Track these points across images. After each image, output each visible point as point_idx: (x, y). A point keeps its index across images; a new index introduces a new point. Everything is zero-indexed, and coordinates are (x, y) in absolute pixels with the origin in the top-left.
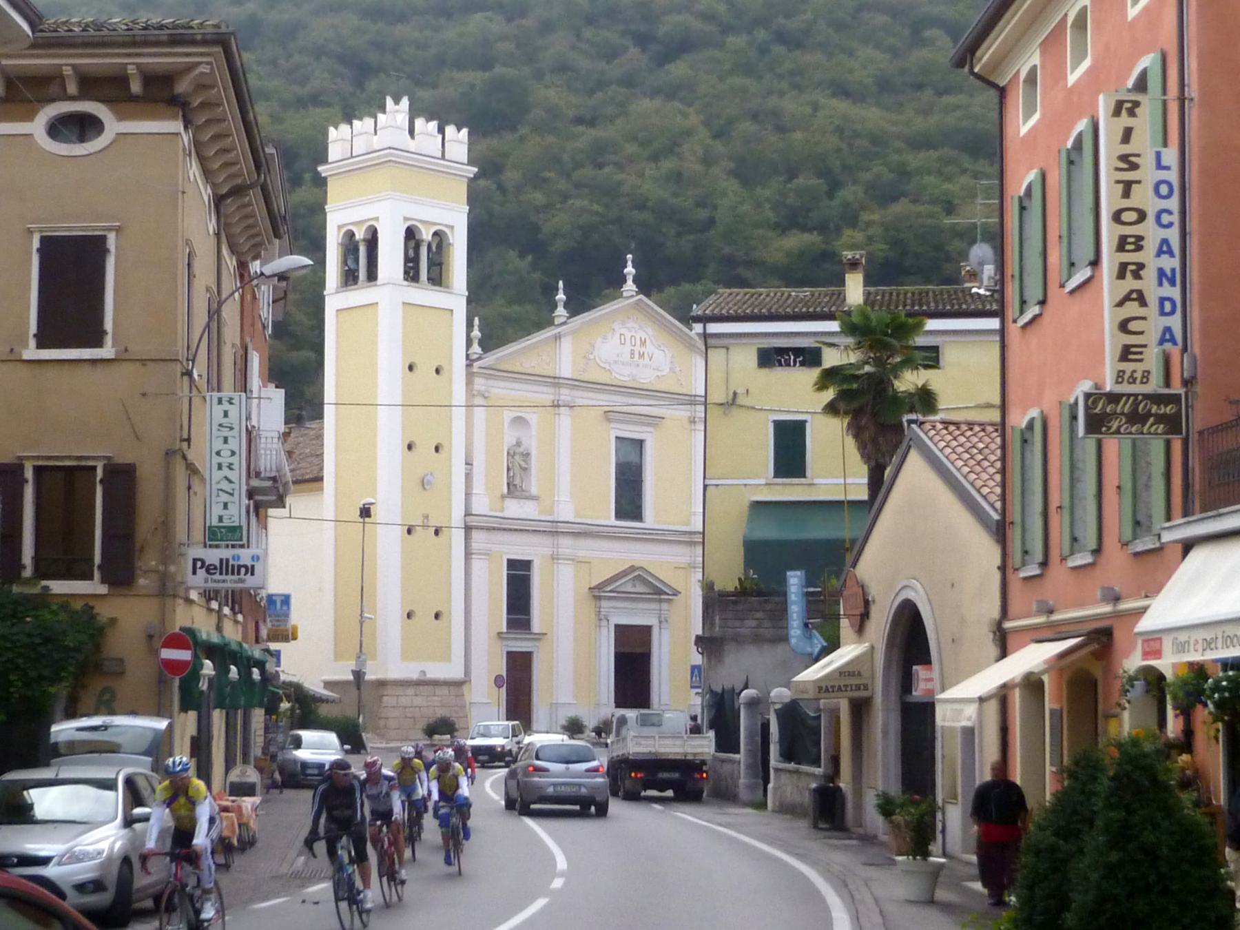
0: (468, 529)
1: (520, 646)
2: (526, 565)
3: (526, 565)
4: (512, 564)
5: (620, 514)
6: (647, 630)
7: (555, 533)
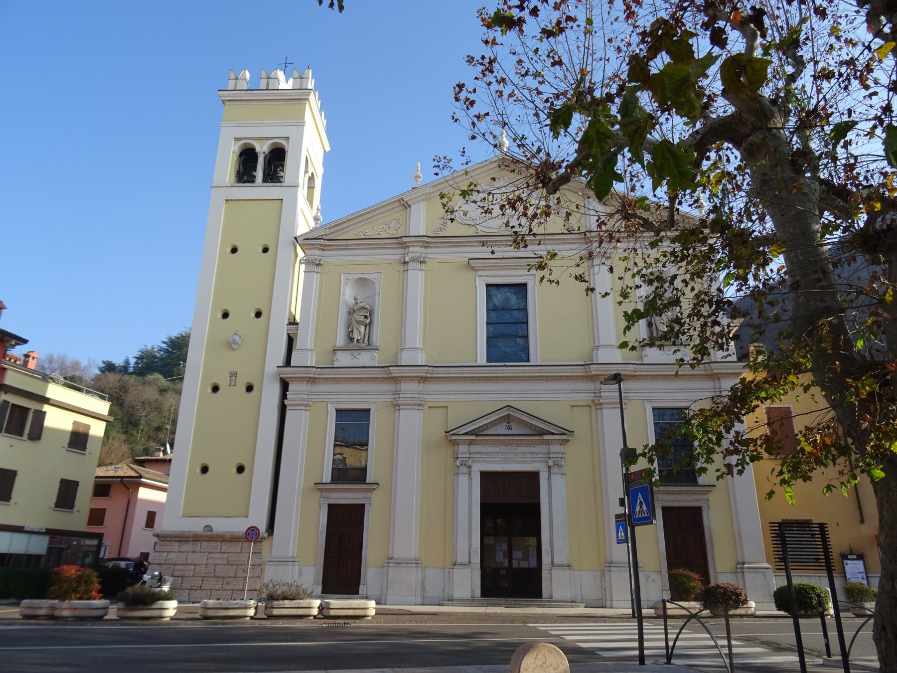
0: (285, 385)
1: (347, 496)
5: (494, 355)
6: (534, 477)
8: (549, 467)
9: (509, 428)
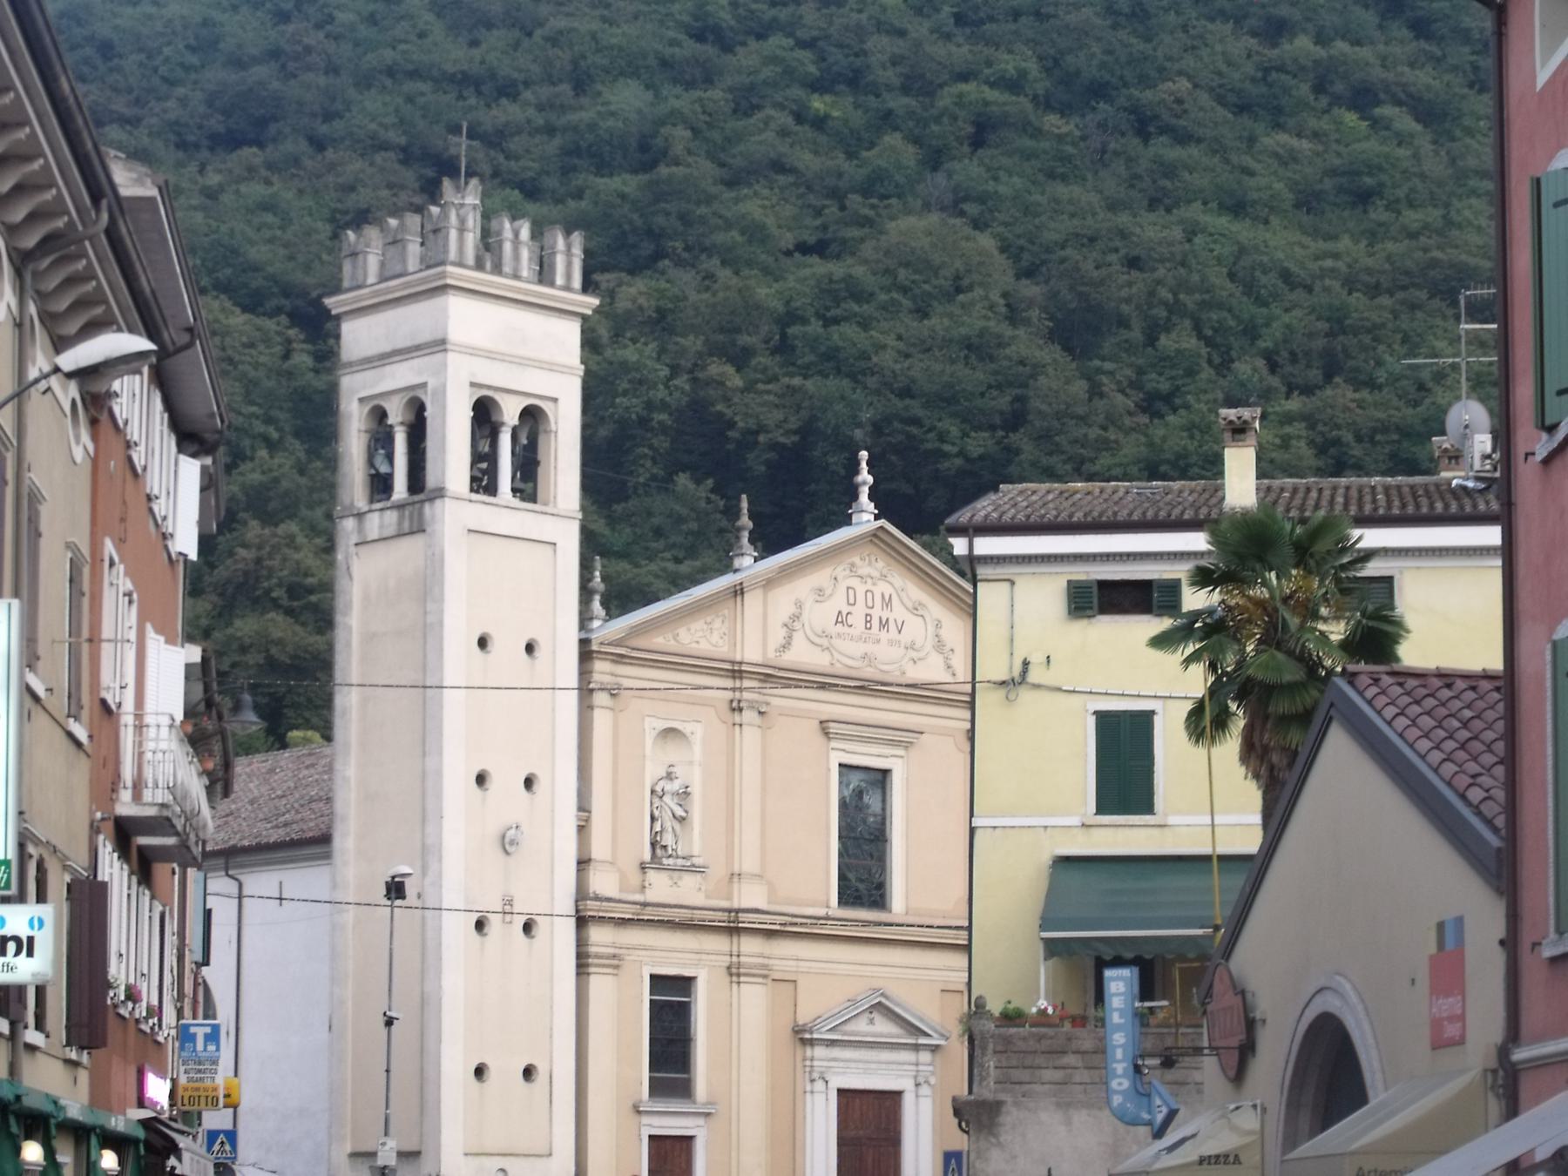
0: (582, 922)
2: (684, 984)
3: (684, 984)
4: (659, 982)
5: (849, 896)
6: (895, 1097)
7: (733, 930)
8: (917, 1085)
9: (871, 1021)
